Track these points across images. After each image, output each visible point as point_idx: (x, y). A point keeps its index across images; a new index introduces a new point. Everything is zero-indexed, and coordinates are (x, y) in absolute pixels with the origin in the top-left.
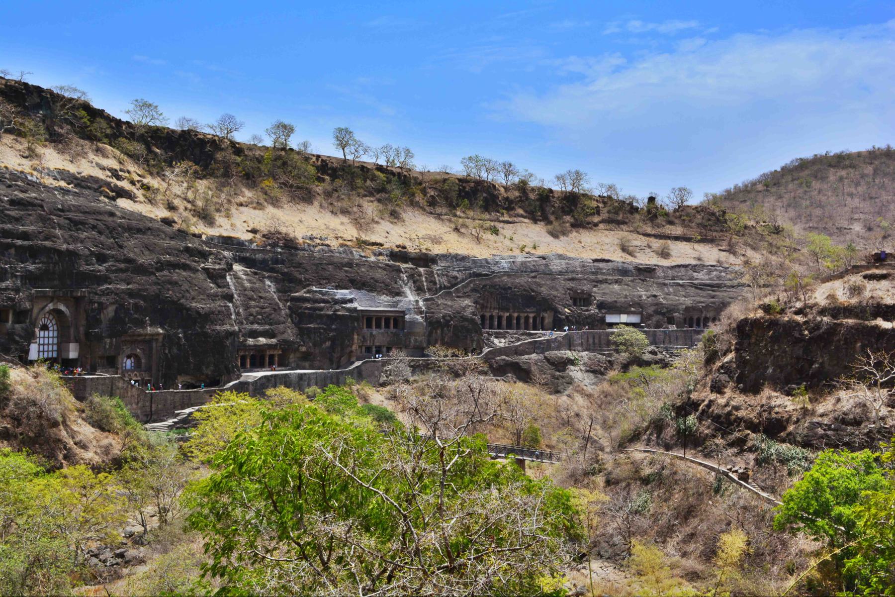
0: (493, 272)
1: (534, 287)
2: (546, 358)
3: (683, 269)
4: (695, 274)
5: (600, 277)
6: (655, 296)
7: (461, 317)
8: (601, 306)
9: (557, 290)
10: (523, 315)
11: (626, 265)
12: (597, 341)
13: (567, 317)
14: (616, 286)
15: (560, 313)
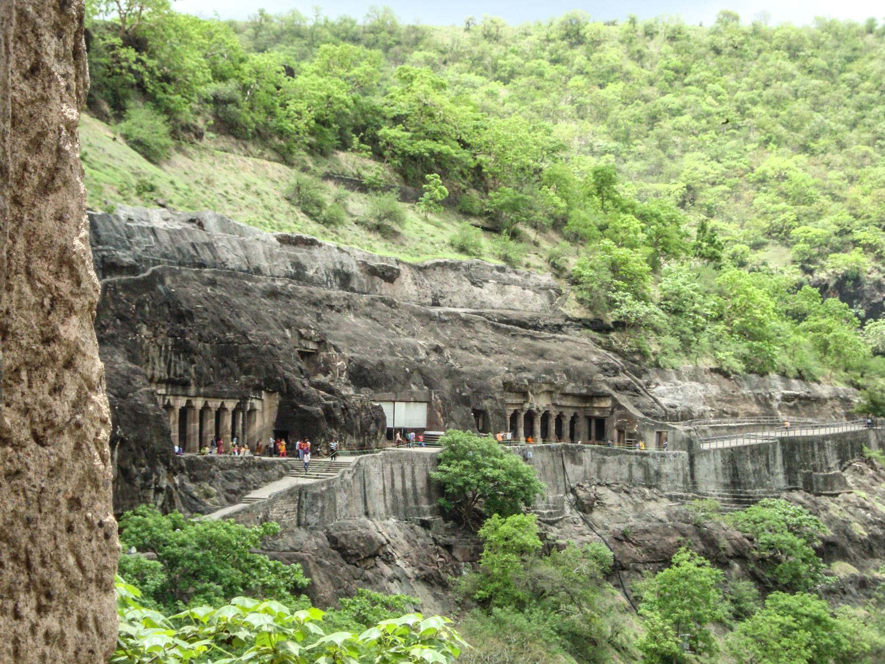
0: (139, 259)
1: (227, 314)
2: (333, 540)
3: (451, 274)
4: (477, 290)
5: (320, 292)
6: (437, 350)
7: (133, 409)
8: (360, 376)
9: (269, 328)
10: (214, 404)
11: (345, 258)
12: (409, 484)
13: (328, 410)
14: (351, 317)
15: (306, 399)
